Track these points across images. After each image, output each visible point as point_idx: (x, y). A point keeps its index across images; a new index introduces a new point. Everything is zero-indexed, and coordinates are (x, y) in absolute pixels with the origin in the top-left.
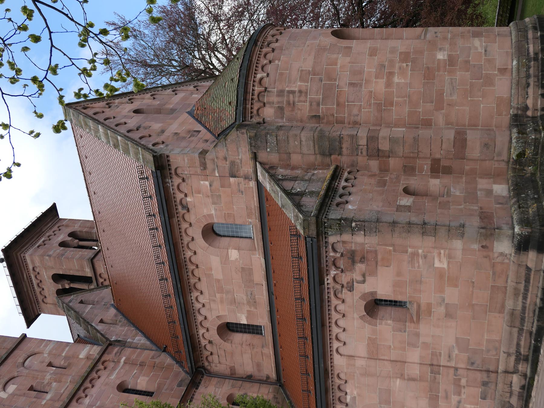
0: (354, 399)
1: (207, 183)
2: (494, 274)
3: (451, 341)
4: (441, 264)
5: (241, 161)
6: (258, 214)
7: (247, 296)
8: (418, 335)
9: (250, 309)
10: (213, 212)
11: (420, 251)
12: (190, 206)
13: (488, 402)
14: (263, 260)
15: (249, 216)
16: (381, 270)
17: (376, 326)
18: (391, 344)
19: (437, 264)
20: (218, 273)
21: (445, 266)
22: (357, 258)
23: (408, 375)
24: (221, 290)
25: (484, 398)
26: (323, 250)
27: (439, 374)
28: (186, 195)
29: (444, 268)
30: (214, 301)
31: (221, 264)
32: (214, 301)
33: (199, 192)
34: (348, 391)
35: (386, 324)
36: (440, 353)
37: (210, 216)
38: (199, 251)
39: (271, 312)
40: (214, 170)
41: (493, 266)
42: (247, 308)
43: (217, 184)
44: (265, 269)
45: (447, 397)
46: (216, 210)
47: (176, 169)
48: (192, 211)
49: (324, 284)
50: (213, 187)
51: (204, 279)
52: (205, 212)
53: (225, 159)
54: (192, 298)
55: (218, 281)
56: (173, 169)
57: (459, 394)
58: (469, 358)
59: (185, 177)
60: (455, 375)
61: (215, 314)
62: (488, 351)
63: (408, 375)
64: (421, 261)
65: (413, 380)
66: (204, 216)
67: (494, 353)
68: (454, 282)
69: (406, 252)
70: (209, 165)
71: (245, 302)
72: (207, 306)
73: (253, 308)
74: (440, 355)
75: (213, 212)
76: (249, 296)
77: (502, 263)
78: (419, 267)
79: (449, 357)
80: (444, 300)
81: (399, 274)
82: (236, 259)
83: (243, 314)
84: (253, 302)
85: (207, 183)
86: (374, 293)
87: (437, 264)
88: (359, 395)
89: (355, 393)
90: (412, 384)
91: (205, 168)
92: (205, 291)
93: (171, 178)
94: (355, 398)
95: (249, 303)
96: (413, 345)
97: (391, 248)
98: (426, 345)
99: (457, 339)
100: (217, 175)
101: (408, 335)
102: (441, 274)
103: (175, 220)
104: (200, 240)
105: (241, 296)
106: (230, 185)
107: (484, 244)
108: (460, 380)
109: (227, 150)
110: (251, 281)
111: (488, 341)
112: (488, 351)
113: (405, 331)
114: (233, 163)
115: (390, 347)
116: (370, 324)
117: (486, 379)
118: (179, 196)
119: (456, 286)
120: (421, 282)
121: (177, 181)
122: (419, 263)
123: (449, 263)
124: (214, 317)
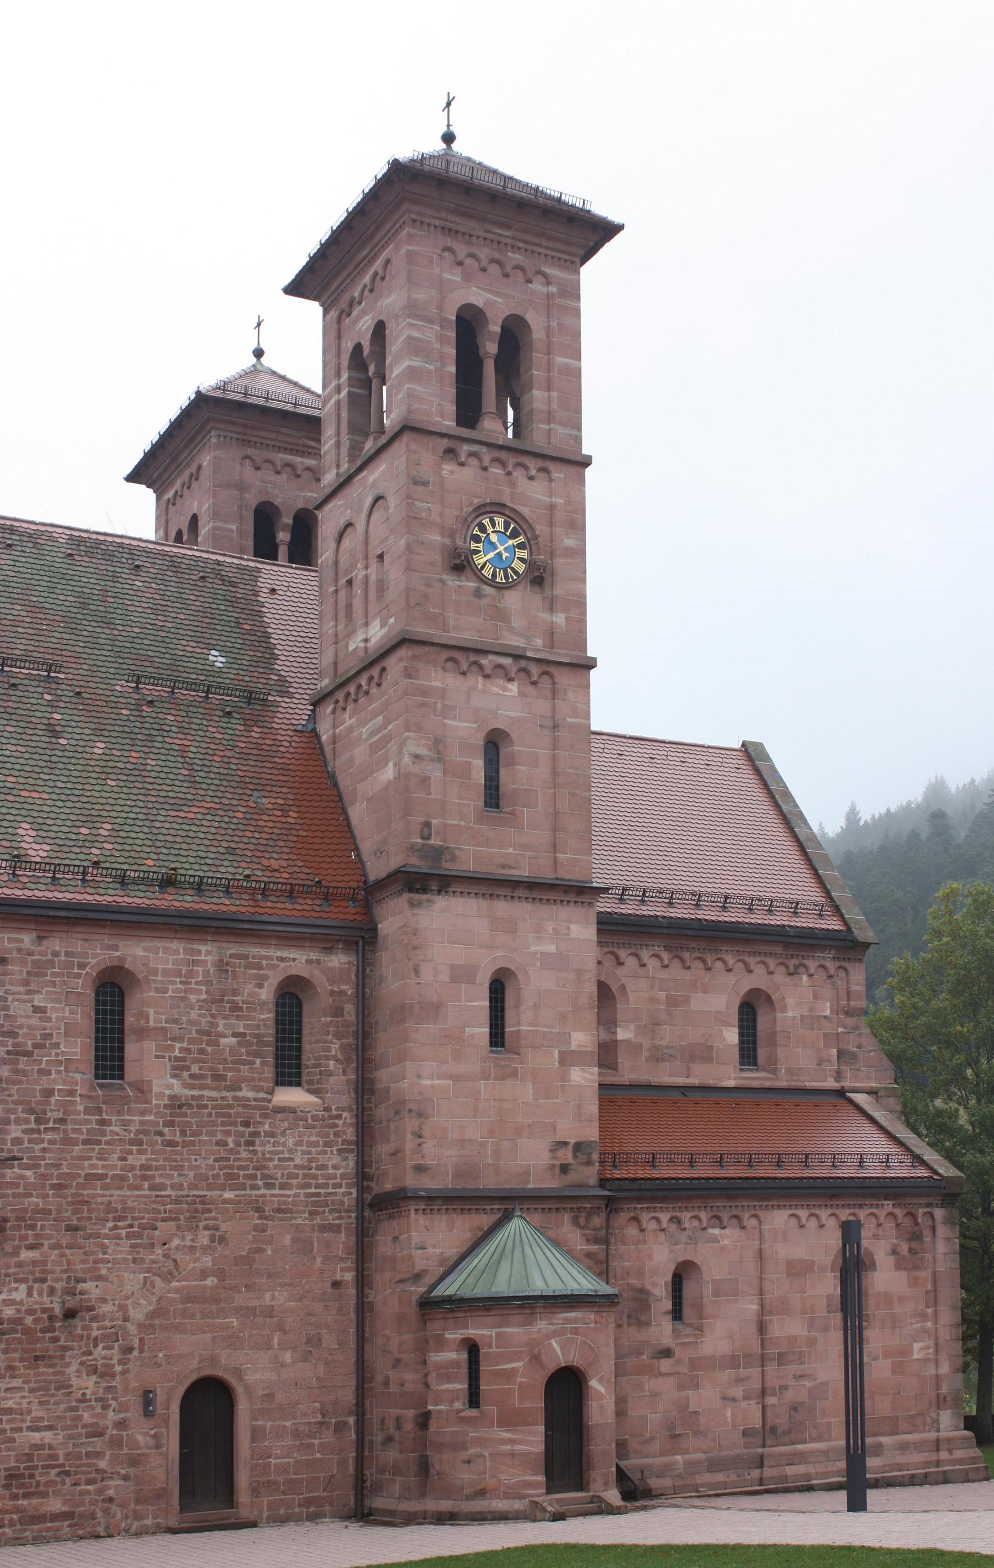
0: (715, 1240)
1: (828, 1013)
2: (912, 1416)
3: (822, 1376)
4: (918, 1351)
5: (859, 1070)
6: (794, 1084)
7: (668, 1047)
8: (826, 1329)
9: (644, 1049)
10: (790, 1014)
11: (929, 1324)
12: (795, 978)
13: (740, 1440)
14: (731, 1083)
15: (789, 1070)
16: (904, 1274)
17: (832, 1271)
18: (808, 1294)
19: (916, 1346)
20: (698, 1002)
21: (916, 1356)
22: (914, 1244)
23: (770, 1321)
24: (672, 1002)
25: (745, 1433)
26: (924, 1200)
27: (779, 1365)
28: (811, 976)
29: (912, 1355)
30: (652, 987)
31: (715, 1012)
32: (652, 987)
33: (815, 997)
34: (727, 1231)
35: (835, 1285)
36: (804, 1363)
37: (784, 1009)
38: (730, 979)
39: (649, 1087)
40: (845, 1027)
41: (921, 1414)
42: (646, 1044)
43: (828, 1028)
44: (719, 1086)
45: (739, 1381)
46: (794, 1018)
47: (845, 969)
48: (788, 979)
49: (885, 1199)
50: (822, 1019)
51: (687, 976)
52: (790, 1001)
53: (859, 1047)
54: (656, 948)
55: (687, 1001)
56: (846, 964)
57: (746, 1398)
58: (801, 1404)
59: (833, 979)
60: (779, 1389)
61: (630, 984)
62: (816, 1427)
63: (770, 1321)
64: (918, 1325)
65: (762, 1328)
66: (783, 999)
67: (814, 1435)
68: (898, 1368)
69: (927, 1307)
70: (850, 1021)
71: (657, 1043)
72: (641, 971)
73: (647, 1054)
74: (801, 1364)
75: (790, 1014)
76: (668, 1052)
77: (924, 1424)
78: (911, 1324)
79: (801, 1376)
80: (874, 1359)
81: (901, 1299)
82: (725, 1039)
83: (636, 1035)
84: (657, 1056)
85: (828, 1013)
86: (873, 1266)
87: (916, 1346)
88: (723, 1248)
89: (726, 1242)
90: (753, 1329)
91: (847, 1013)
92: (663, 974)
93: (834, 958)
94: (718, 1242)
95: (657, 1048)
96: (811, 1326)
97: (929, 1287)
98: (812, 1342)
99: (826, 1383)
100: (840, 1030)
101: (824, 1317)
102: (905, 1352)
103: (779, 949)
104: (747, 984)
105: (667, 1037)
106: (827, 1047)
107: (948, 1398)
108: (774, 1395)
109: (870, 1051)
110: (693, 1058)
111: (829, 1423)
112: (816, 1427)
113: (828, 1312)
114: (854, 1056)
115: (805, 1292)
116: (833, 1262)
117: (780, 1431)
118: (812, 965)
119: (894, 1373)
120: (894, 1328)
121: (831, 966)
122: (917, 1323)
123: (918, 1360)
124: (624, 981)
